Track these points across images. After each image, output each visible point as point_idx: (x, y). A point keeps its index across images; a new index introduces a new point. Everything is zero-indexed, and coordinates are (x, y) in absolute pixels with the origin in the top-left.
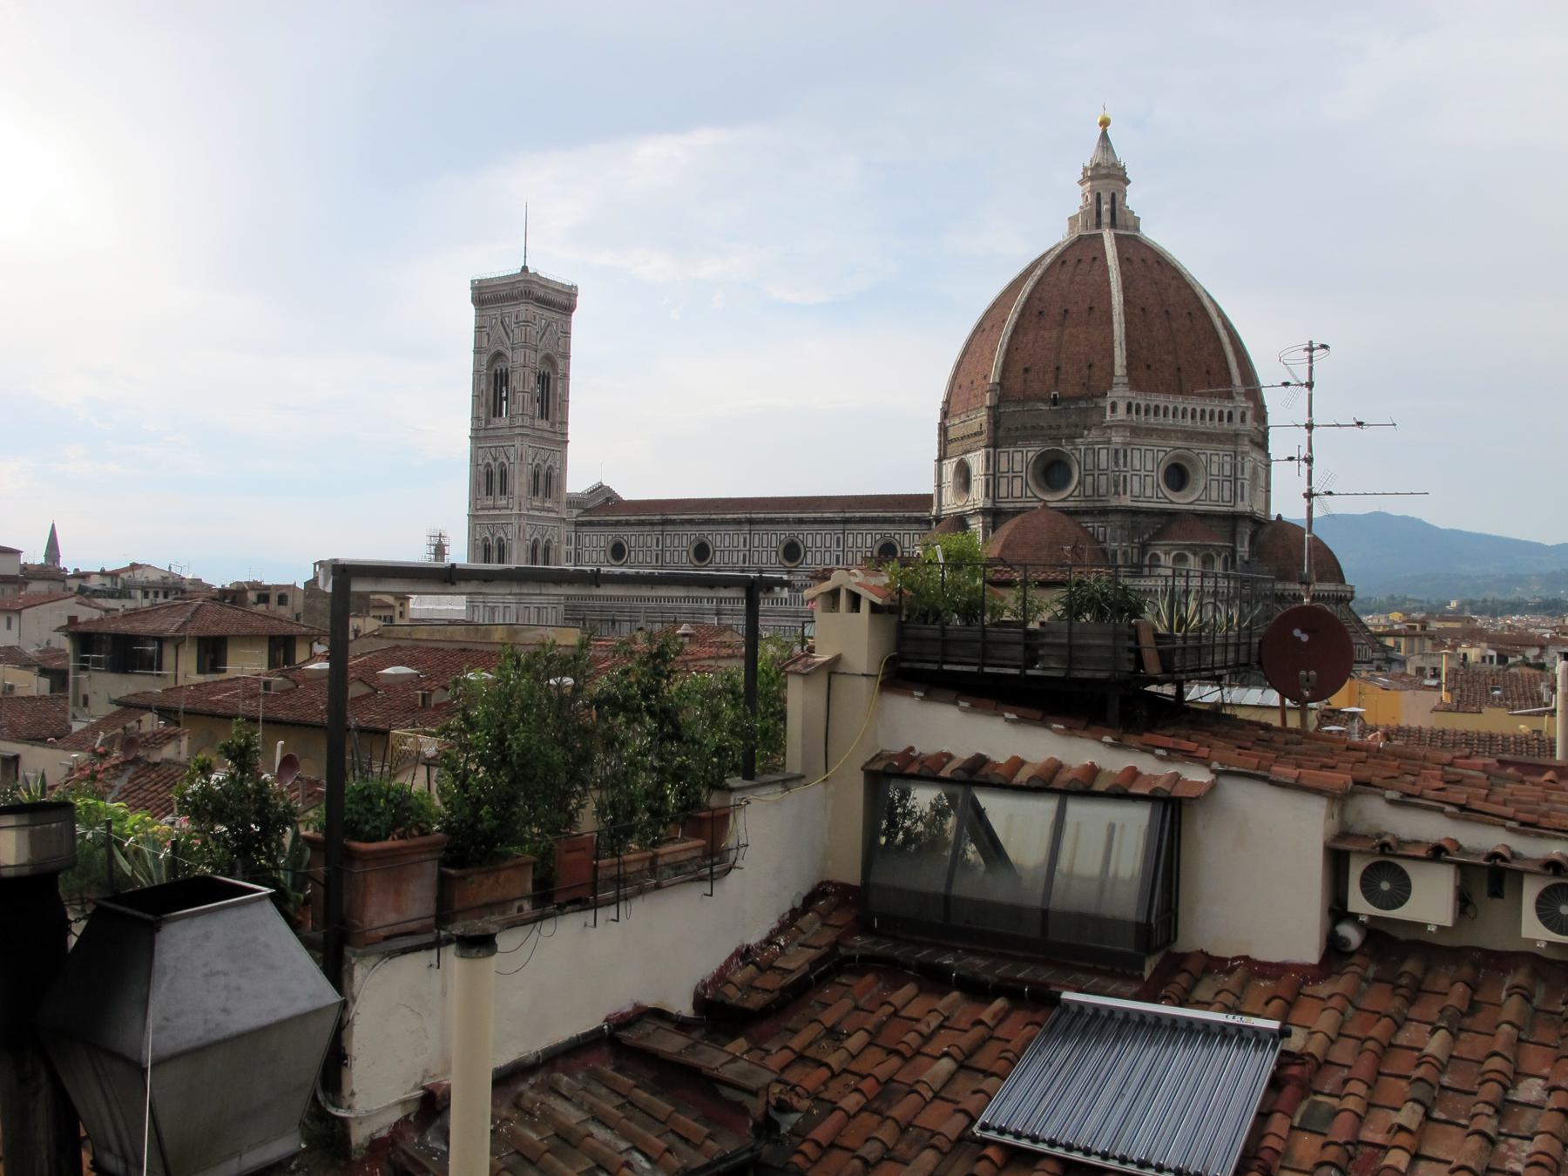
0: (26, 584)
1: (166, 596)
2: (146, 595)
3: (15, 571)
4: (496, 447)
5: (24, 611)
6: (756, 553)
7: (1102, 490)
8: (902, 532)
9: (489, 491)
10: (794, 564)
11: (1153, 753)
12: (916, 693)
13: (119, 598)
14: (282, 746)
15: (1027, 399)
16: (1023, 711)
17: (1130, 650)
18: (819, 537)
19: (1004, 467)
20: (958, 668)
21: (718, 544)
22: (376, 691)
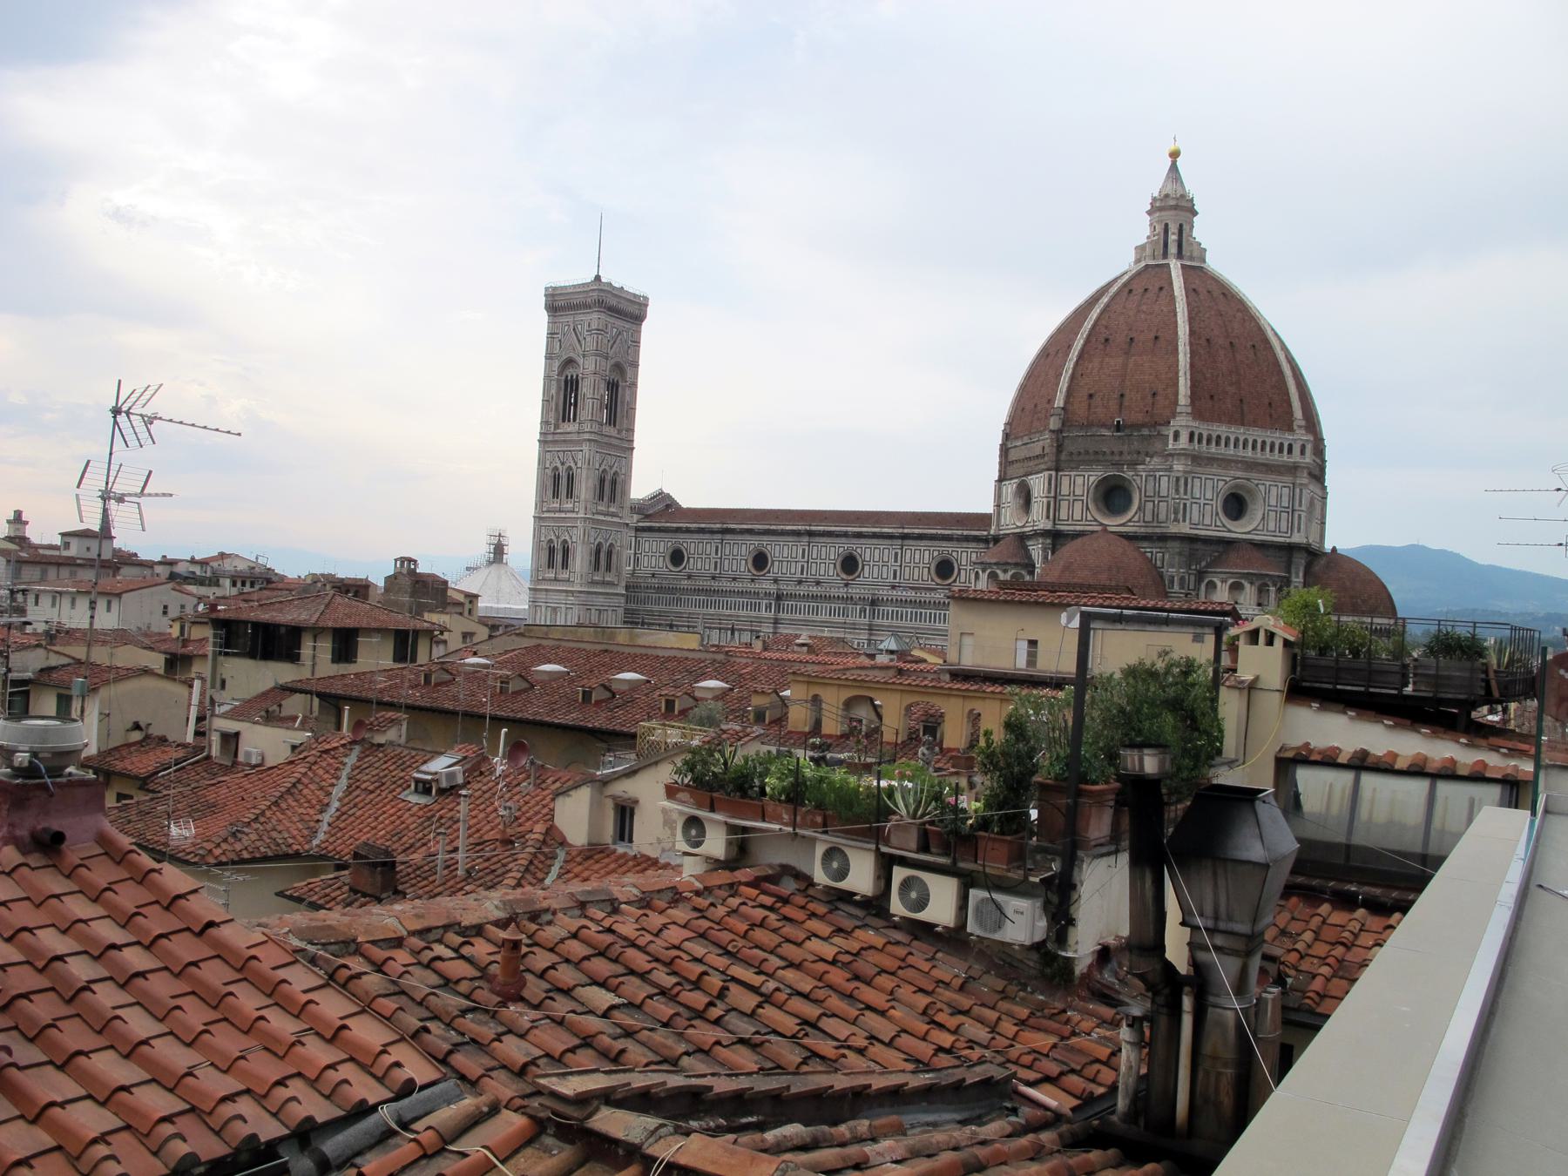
0: (119, 568)
1: (252, 585)
2: (234, 584)
3: (106, 555)
4: (564, 451)
5: (124, 595)
6: (814, 565)
7: (1162, 517)
8: (959, 550)
9: (556, 494)
10: (851, 577)
11: (1498, 751)
12: (1313, 705)
13: (210, 585)
14: (506, 733)
15: (1090, 425)
16: (1399, 720)
17: (1483, 680)
18: (877, 551)
19: (1065, 490)
20: (1349, 688)
21: (777, 555)
22: (533, 686)
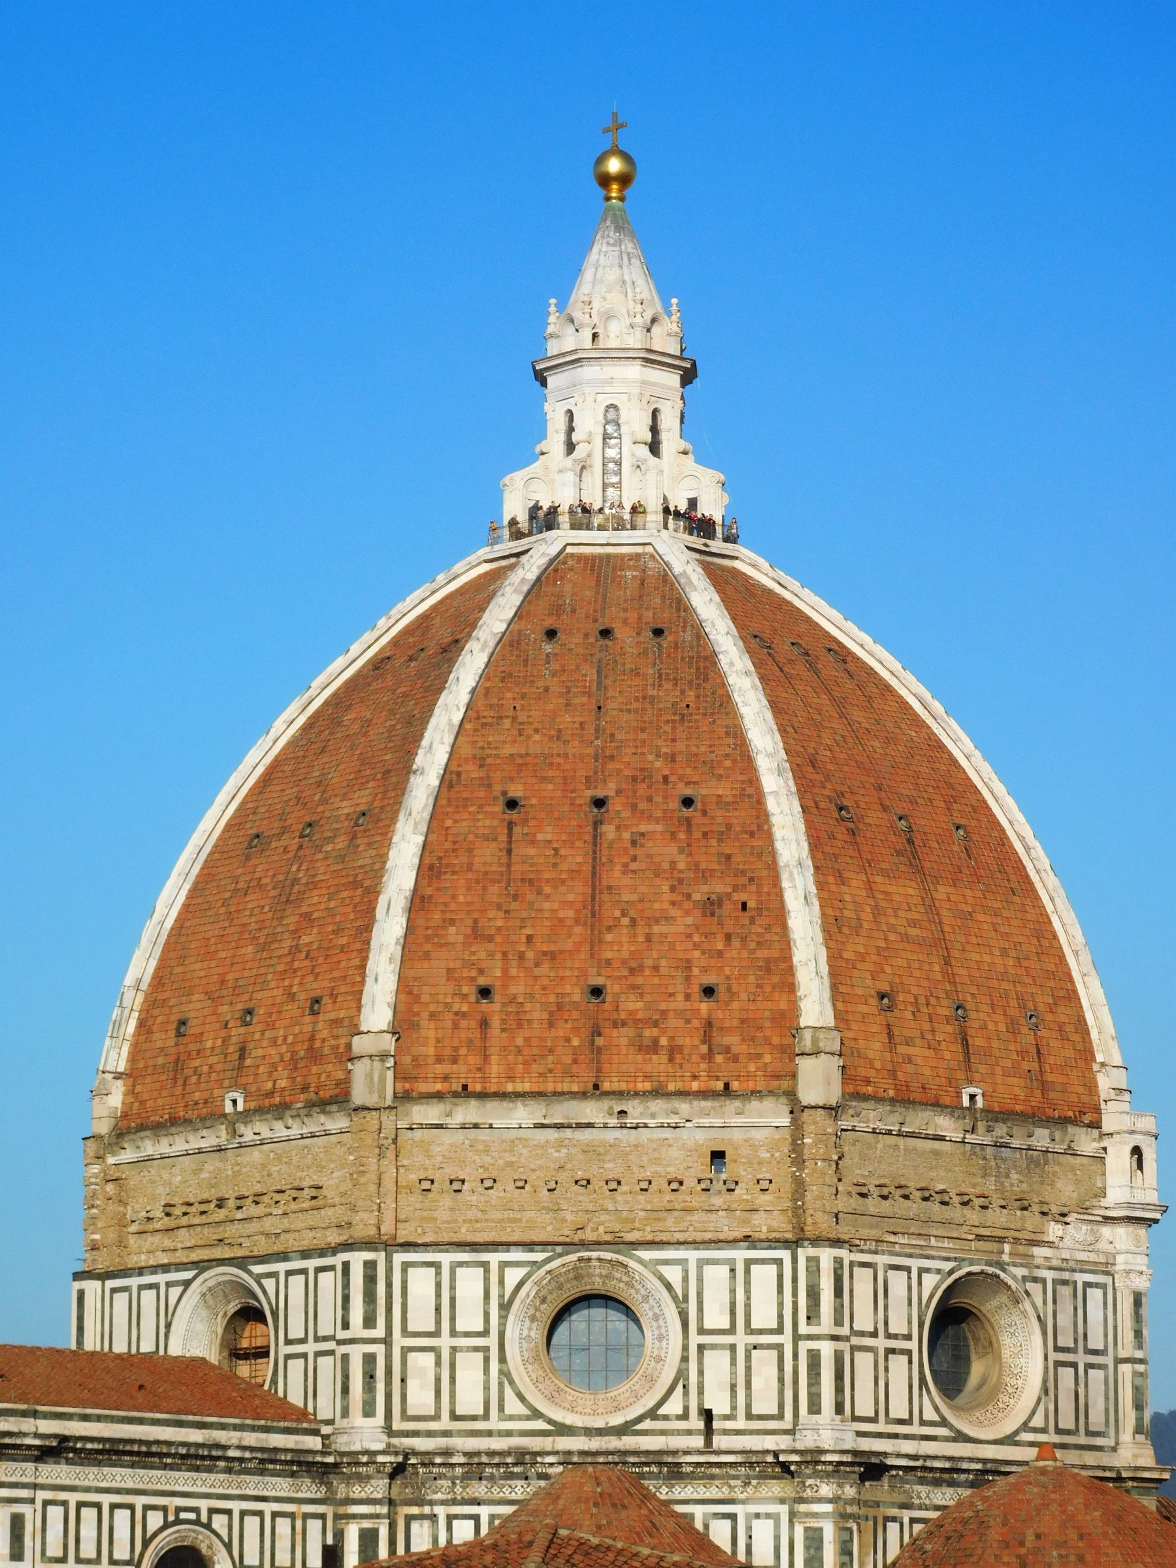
8: (236, 1506)
